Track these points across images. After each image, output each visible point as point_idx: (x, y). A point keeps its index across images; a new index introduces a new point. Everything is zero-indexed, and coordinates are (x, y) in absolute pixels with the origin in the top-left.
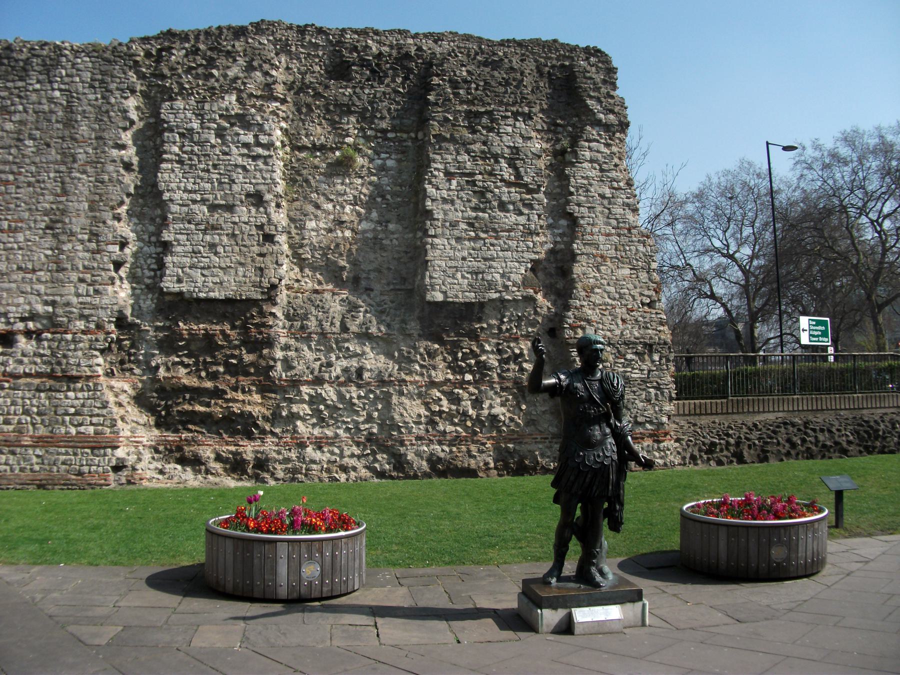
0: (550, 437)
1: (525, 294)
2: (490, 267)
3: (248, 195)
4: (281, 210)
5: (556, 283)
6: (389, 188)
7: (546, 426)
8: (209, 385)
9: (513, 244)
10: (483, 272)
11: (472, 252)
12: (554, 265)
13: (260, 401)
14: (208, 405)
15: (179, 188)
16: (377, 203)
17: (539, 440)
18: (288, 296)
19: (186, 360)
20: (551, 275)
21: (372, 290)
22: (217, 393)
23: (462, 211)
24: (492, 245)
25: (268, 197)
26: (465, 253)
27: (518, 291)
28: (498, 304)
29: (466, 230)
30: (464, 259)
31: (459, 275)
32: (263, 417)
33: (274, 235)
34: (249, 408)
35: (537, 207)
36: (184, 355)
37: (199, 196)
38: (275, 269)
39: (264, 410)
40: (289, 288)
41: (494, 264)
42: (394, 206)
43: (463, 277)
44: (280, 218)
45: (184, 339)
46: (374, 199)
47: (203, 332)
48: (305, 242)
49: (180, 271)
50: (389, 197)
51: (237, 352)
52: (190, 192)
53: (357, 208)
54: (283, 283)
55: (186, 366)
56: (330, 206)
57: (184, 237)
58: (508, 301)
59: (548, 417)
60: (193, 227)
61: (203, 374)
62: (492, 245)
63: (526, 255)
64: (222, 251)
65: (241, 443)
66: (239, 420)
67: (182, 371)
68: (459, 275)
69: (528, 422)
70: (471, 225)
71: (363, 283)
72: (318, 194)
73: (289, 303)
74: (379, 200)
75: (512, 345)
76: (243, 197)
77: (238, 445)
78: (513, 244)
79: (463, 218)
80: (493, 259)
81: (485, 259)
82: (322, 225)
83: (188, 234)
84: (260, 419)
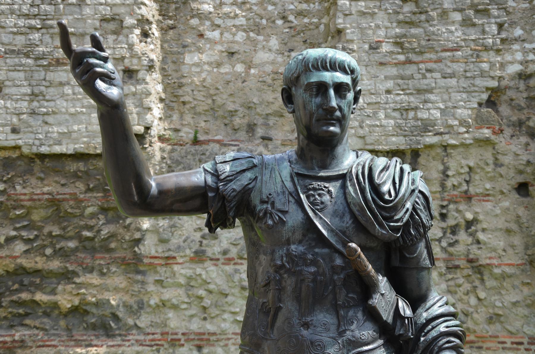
0: (525, 340)
1: (477, 135)
2: (426, 102)
3: (104, 20)
4: (149, 40)
5: (529, 119)
6: (292, 7)
7: (518, 324)
8: (55, 265)
9: (459, 67)
10: (416, 109)
11: (400, 81)
12: (525, 95)
13: (122, 286)
14: (53, 292)
15: (12, 12)
16: (277, 27)
17: (508, 345)
18: (162, 150)
19: (24, 233)
20: (520, 109)
21: (270, 139)
22: (67, 276)
23: (387, 28)
24: (429, 71)
25: (129, 21)
26: (390, 84)
27: (467, 132)
28: (439, 150)
29: (392, 53)
30: (388, 92)
31: (382, 115)
32: (125, 305)
33: (137, 71)
34: (106, 295)
35: (495, 13)
36: (24, 227)
37: (38, 21)
38: (138, 114)
39: (126, 298)
40: (161, 139)
41: (432, 97)
42: (298, 28)
43: (387, 117)
44: (152, 51)
45: (23, 207)
46: (274, 22)
47: (46, 196)
48: (184, 81)
49: (15, 120)
50: (291, 18)
51: (92, 223)
52: (27, 16)
53: (252, 34)
54: (154, 132)
55: (28, 241)
56: (216, 34)
57: (22, 75)
58: (454, 147)
59: (522, 311)
60: (30, 61)
61: (49, 251)
62: (429, 71)
63: (478, 82)
64: (70, 91)
65: (95, 342)
66: (94, 310)
67: (20, 247)
68: (382, 115)
69: (491, 318)
70: (396, 44)
71: (260, 132)
72: (200, 18)
73: (163, 158)
74: (280, 22)
75: (462, 207)
76: (98, 24)
77: (91, 345)
78: (459, 67)
79: (386, 37)
80: (430, 91)
81: (419, 91)
82: (204, 58)
83: (25, 71)
84: (121, 309)
